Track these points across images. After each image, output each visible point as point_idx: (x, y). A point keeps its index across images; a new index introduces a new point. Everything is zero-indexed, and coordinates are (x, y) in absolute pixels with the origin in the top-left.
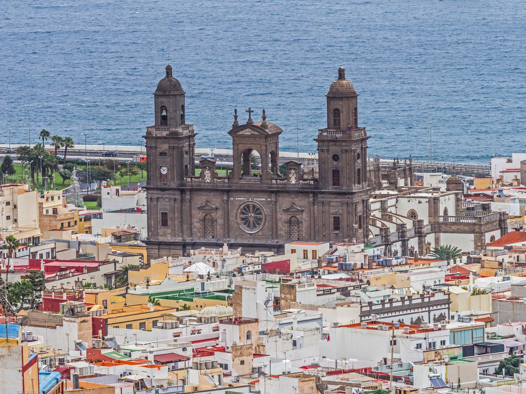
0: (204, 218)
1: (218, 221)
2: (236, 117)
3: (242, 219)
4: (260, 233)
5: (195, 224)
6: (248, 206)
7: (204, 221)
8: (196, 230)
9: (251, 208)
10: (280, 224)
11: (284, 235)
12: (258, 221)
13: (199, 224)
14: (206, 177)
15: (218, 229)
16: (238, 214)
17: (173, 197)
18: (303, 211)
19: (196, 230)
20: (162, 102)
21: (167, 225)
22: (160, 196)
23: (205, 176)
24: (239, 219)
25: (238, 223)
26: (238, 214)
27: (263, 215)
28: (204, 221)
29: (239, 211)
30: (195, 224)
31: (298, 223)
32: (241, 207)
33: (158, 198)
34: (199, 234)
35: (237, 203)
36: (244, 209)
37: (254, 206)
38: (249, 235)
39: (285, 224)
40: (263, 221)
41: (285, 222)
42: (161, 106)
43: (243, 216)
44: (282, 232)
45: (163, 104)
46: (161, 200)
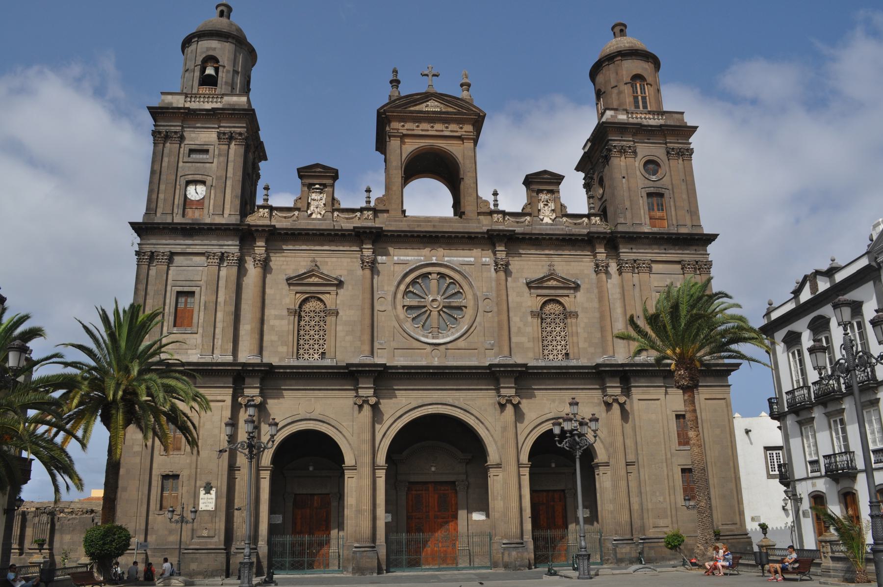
0: (300, 306)
1: (341, 313)
2: (395, 83)
3: (410, 308)
4: (461, 343)
5: (272, 322)
6: (425, 276)
7: (300, 317)
8: (274, 338)
9: (434, 283)
10: (515, 320)
11: (530, 345)
12: (452, 310)
13: (285, 322)
14: (312, 208)
15: (340, 334)
16: (400, 295)
17: (216, 250)
18: (577, 287)
19: (274, 338)
20: (208, 49)
21: (190, 325)
22: (178, 249)
23: (309, 204)
24: (399, 307)
25: (397, 318)
26: (400, 295)
27: (470, 296)
28: (300, 317)
29: (402, 287)
30: (272, 322)
31: (567, 315)
32: (408, 279)
33: (172, 254)
34: (283, 349)
35: (397, 267)
36: (414, 282)
37: (442, 276)
38: (429, 348)
39: (529, 319)
40: (469, 313)
41: (533, 314)
42: (204, 56)
43: (414, 302)
44: (524, 339)
45: (211, 53)
46: (178, 260)
